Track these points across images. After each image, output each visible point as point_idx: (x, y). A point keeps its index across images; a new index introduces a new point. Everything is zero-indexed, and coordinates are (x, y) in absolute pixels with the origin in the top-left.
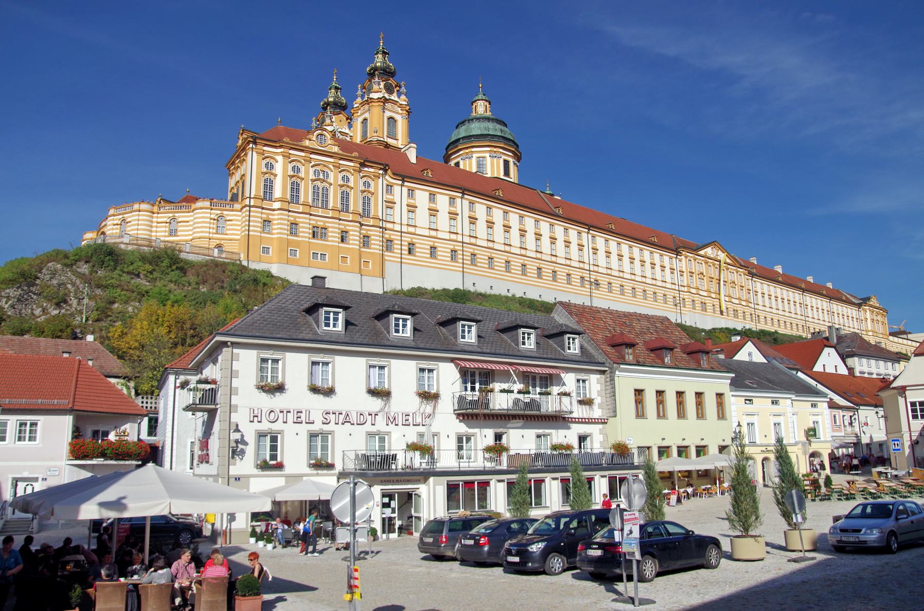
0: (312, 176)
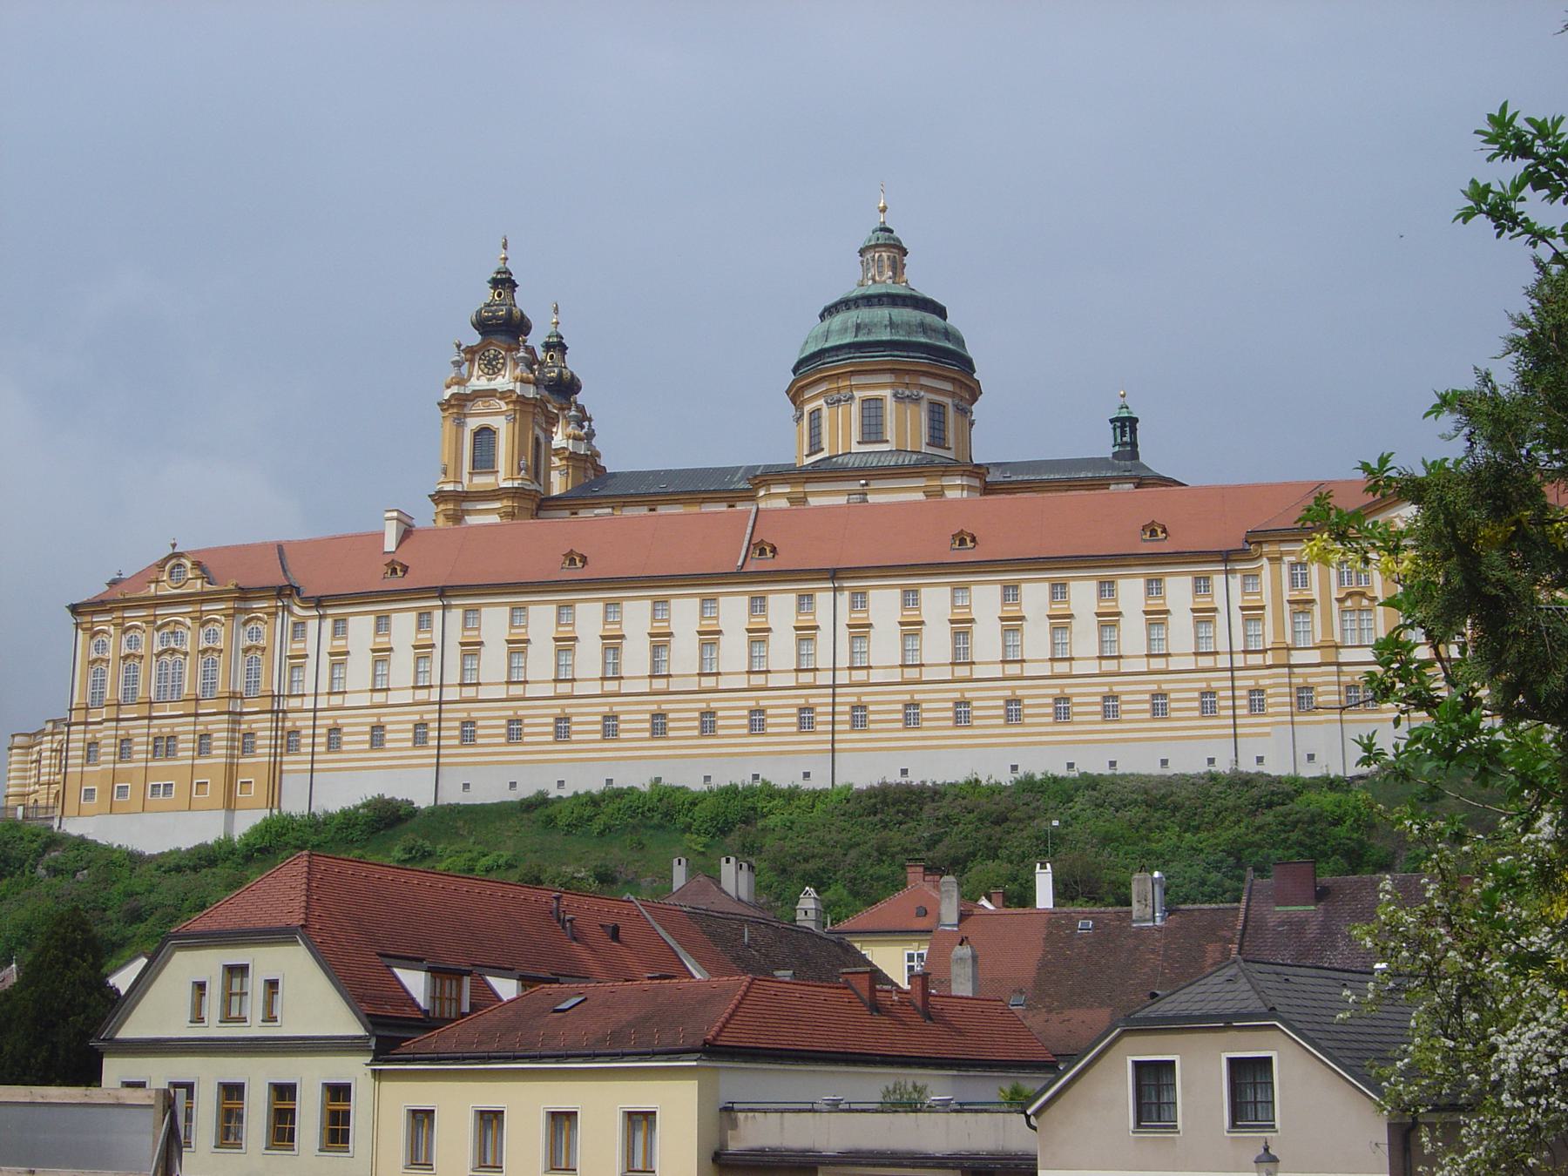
0: (158, 648)
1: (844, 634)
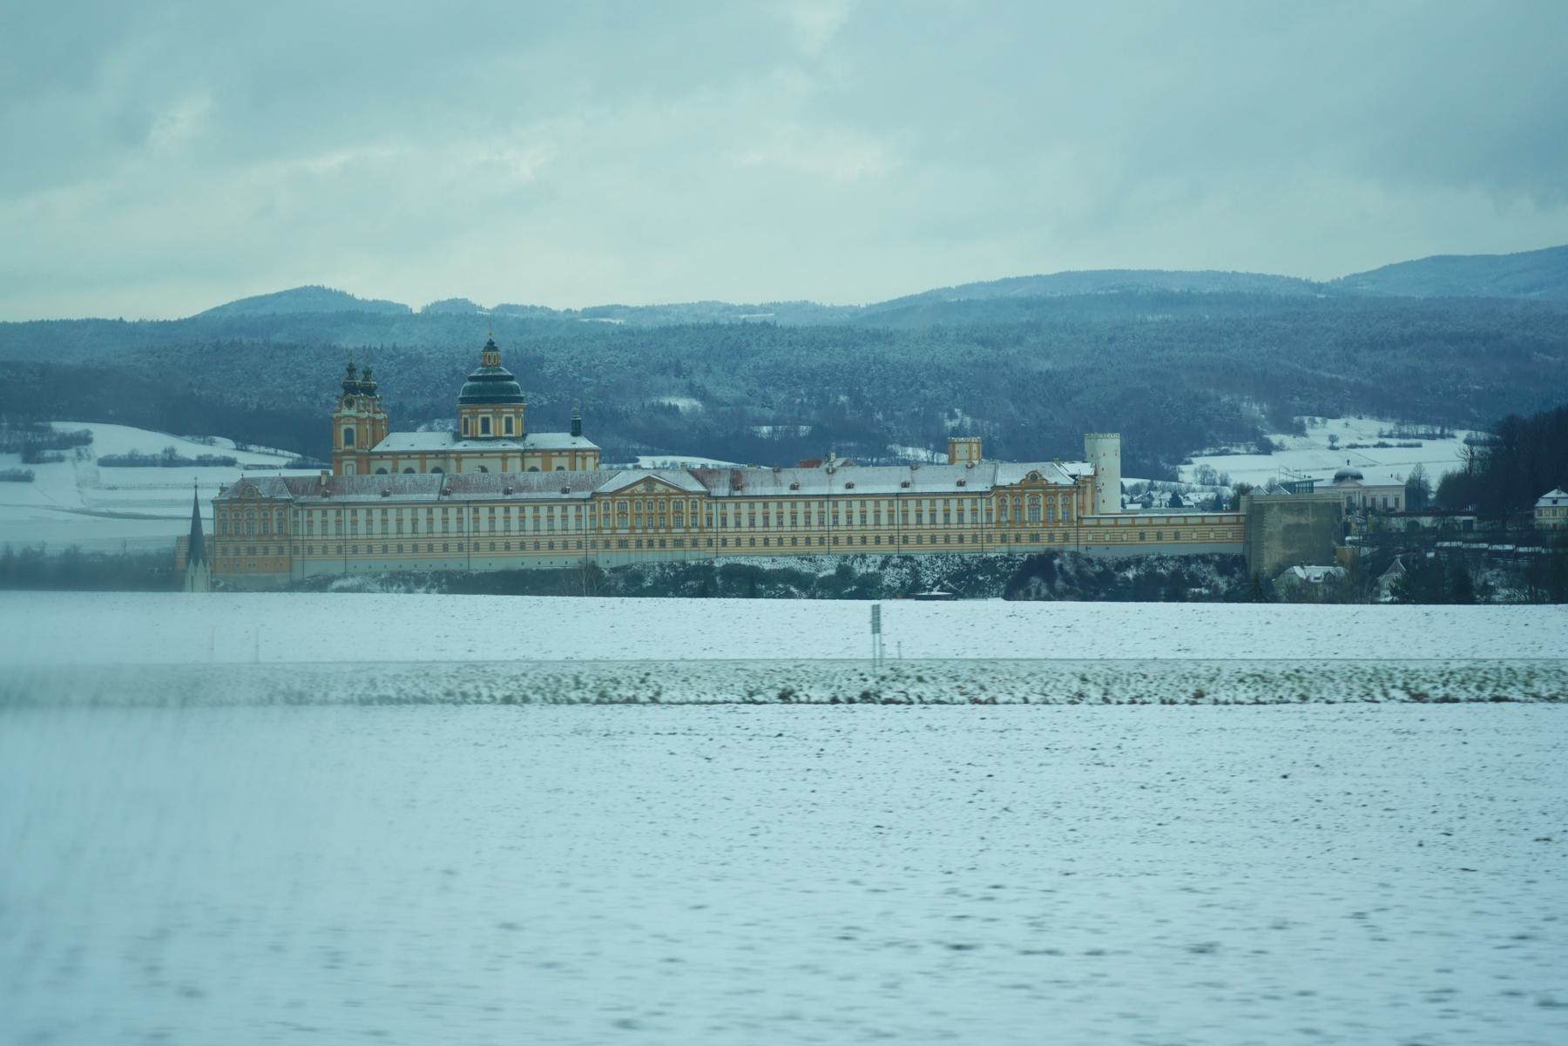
1: (471, 521)
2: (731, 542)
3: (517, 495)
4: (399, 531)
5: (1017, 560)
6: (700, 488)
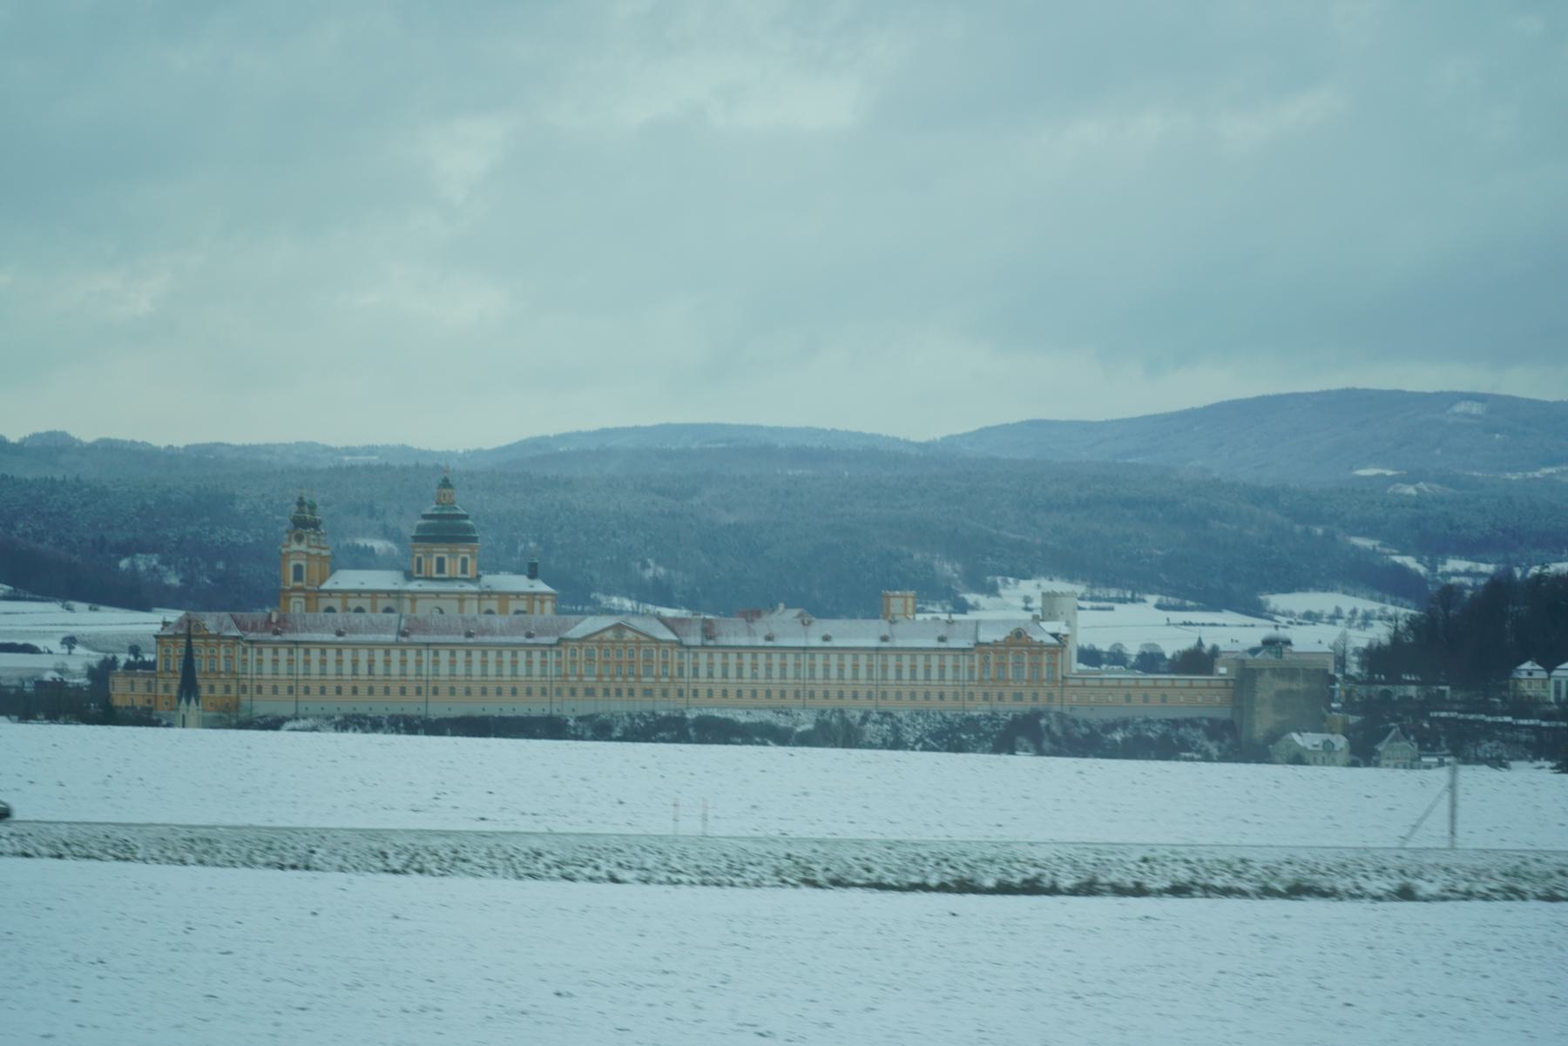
2: (703, 692)
3: (479, 639)
4: (355, 673)
5: (1002, 719)
6: (672, 637)
